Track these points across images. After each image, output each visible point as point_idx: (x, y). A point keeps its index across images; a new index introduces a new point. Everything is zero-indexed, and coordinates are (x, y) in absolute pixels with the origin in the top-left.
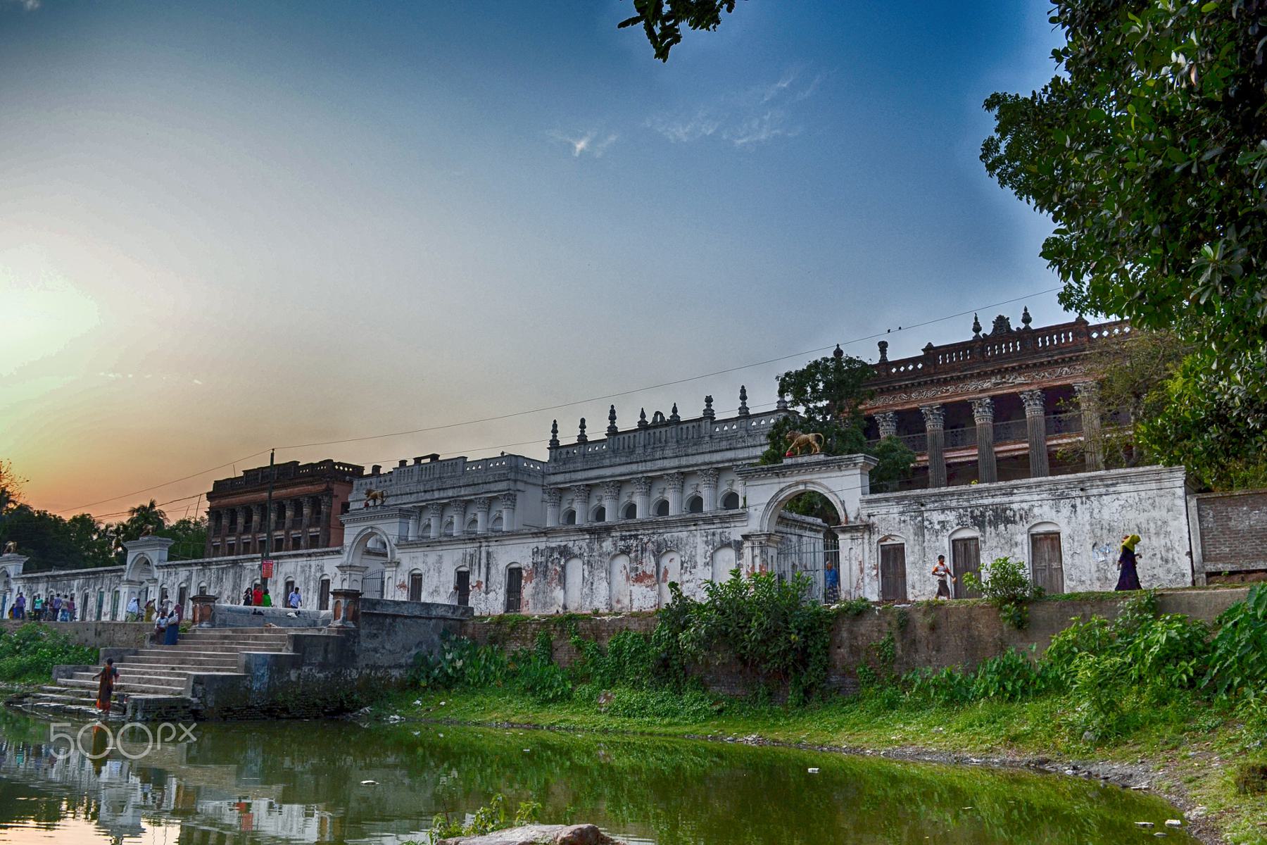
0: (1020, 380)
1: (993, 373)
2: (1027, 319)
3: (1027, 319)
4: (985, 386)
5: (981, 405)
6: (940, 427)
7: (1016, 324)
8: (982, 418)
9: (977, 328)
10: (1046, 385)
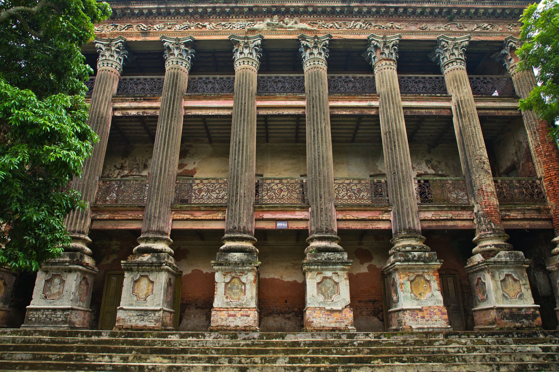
1: (270, 13)
4: (256, 27)
5: (246, 46)
10: (335, 36)
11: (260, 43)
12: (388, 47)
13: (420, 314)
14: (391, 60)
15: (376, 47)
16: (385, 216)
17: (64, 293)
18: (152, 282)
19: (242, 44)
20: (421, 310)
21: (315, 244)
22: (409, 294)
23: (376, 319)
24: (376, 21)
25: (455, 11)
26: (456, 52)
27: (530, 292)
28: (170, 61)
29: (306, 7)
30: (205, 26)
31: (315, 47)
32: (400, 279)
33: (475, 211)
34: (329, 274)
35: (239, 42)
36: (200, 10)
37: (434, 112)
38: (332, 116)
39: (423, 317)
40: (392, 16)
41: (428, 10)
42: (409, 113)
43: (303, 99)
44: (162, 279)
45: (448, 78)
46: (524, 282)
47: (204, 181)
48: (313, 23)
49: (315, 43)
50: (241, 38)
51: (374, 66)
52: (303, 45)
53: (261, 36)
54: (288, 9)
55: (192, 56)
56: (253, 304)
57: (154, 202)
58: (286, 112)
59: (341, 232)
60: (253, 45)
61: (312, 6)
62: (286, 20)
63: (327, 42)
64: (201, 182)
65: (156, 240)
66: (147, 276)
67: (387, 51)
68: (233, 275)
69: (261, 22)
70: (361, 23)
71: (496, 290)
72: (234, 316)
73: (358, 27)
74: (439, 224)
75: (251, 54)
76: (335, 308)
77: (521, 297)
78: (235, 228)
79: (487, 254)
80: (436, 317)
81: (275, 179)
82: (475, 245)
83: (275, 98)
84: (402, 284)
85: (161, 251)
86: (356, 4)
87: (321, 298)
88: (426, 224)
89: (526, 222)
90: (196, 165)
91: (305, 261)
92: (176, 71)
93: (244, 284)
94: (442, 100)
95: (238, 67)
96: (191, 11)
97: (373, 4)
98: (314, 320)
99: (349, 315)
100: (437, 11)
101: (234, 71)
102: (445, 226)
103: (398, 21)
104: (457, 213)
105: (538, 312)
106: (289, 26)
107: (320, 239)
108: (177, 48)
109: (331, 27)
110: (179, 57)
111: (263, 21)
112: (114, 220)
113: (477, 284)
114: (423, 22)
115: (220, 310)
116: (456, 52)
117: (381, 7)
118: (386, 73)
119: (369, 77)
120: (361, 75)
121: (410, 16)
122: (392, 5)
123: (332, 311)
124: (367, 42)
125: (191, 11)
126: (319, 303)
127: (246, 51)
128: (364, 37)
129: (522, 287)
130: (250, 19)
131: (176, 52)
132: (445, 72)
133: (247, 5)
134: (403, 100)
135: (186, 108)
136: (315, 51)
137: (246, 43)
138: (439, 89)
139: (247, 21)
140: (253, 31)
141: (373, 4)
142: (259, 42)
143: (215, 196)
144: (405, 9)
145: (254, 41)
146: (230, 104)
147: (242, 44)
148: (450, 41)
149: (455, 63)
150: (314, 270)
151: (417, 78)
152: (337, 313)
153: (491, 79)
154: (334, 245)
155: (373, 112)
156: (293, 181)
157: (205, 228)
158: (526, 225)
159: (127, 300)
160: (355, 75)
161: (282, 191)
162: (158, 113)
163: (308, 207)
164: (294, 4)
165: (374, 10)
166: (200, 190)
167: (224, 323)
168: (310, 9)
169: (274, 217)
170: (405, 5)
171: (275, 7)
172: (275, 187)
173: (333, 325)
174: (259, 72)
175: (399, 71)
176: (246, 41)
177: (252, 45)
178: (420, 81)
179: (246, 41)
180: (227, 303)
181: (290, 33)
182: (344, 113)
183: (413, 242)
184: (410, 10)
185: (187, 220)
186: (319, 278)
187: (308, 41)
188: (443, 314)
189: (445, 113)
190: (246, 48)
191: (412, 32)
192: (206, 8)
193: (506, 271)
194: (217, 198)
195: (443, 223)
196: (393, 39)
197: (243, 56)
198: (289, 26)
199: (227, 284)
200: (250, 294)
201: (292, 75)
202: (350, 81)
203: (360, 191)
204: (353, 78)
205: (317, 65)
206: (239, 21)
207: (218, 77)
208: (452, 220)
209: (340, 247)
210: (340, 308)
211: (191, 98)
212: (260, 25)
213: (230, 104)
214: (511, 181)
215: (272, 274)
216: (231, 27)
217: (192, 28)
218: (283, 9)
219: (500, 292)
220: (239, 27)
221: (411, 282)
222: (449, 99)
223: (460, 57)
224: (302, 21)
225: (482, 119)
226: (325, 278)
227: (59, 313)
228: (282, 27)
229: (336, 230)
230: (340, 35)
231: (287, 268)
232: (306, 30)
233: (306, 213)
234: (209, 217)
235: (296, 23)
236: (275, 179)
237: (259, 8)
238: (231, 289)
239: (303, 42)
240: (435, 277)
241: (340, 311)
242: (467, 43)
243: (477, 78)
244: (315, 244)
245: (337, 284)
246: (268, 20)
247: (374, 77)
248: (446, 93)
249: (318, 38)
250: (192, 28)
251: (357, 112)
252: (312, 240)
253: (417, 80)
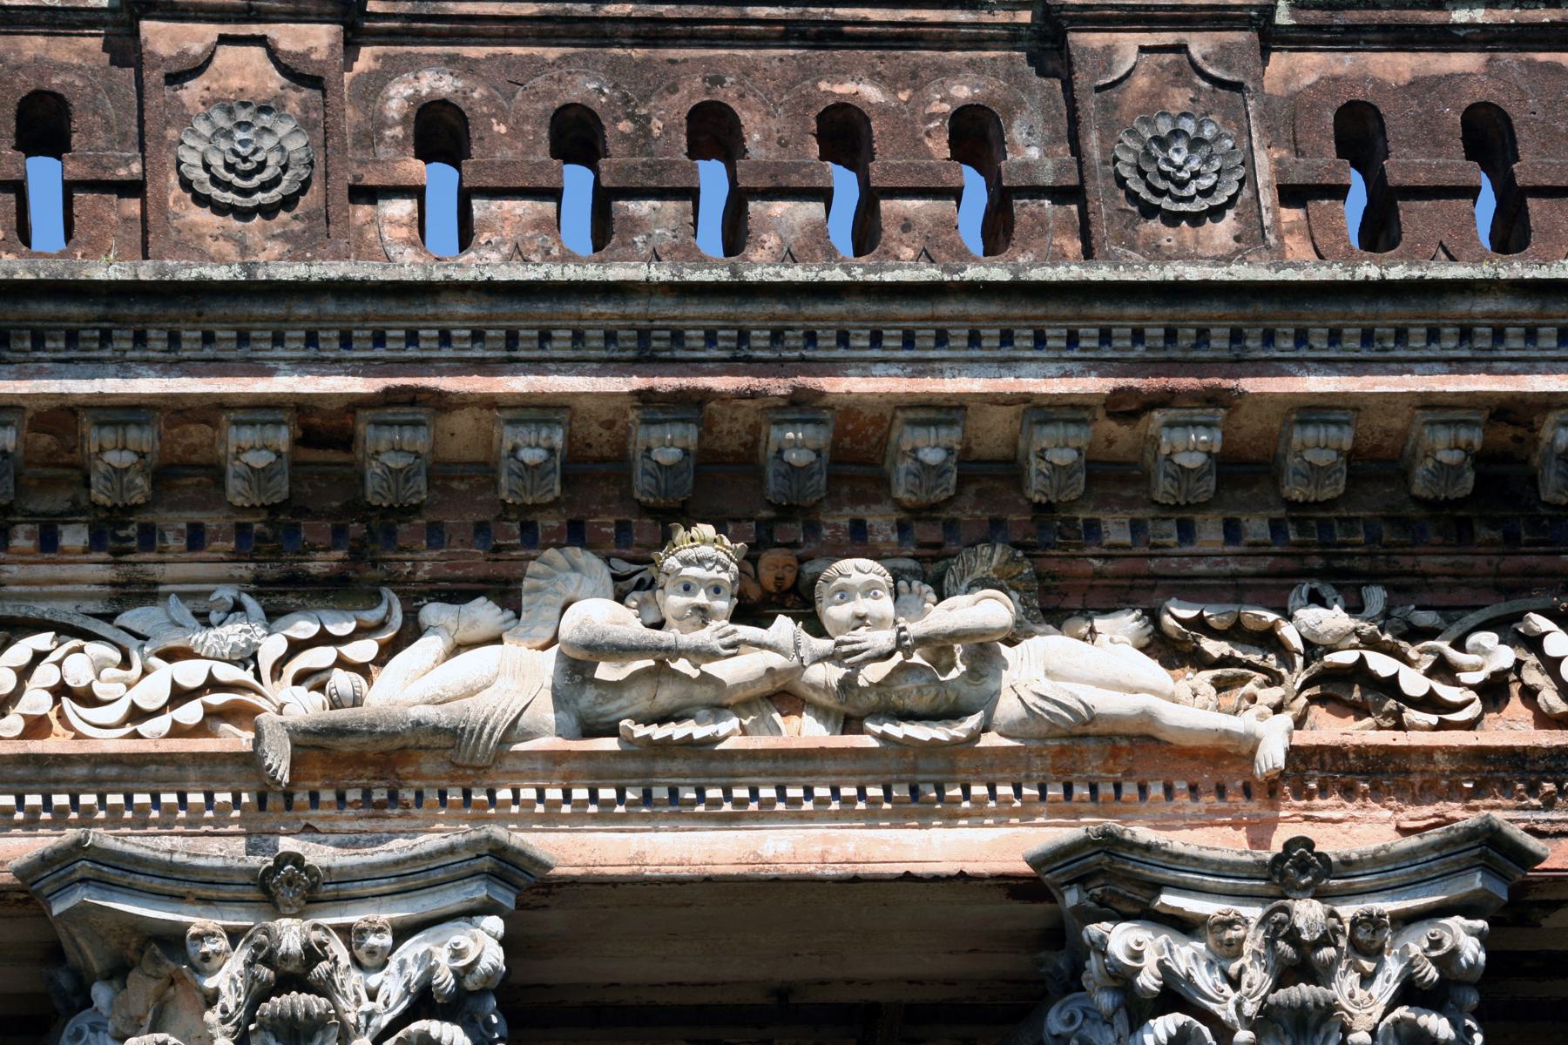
0: (1097, 667)
11: (492, 956)
29: (1123, 407)
35: (173, 941)
48: (1236, 633)
52: (1122, 979)
53: (506, 866)
60: (393, 986)
61: (1213, 398)
63: (1465, 938)
69: (484, 614)
109: (1494, 691)
111: (507, 595)
130: (318, 565)
139: (259, 587)
142: (484, 944)
145: (402, 932)
147: (228, 977)
171: (691, 404)
176: (291, 934)
179: (291, 934)
187: (1185, 926)
212: (472, 674)
216: (36, 700)
218: (797, 442)
220: (152, 692)
237: (462, 422)
239: (1121, 938)
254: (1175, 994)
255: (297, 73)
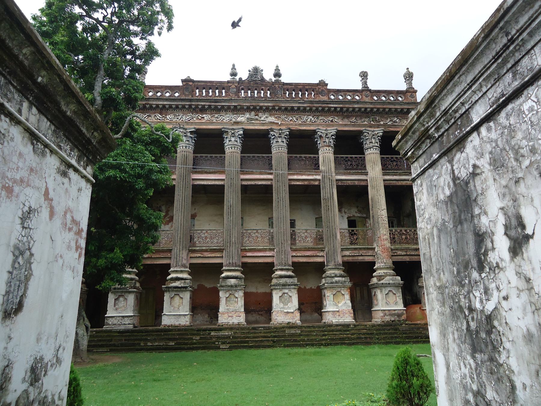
0: (272, 119)
1: (249, 109)
2: (277, 74)
3: (277, 74)
4: (239, 119)
5: (233, 135)
6: (191, 149)
7: (268, 76)
8: (232, 146)
9: (234, 74)
10: (294, 128)
12: (328, 138)
13: (338, 314)
14: (329, 146)
15: (321, 136)
16: (321, 254)
17: (128, 306)
18: (182, 298)
19: (230, 134)
20: (338, 311)
21: (279, 273)
22: (332, 303)
23: (316, 314)
24: (322, 116)
25: (375, 110)
26: (373, 141)
27: (402, 300)
28: (181, 145)
29: (274, 106)
30: (203, 118)
31: (280, 137)
32: (328, 294)
33: (376, 250)
34: (286, 291)
36: (200, 107)
37: (356, 183)
38: (291, 186)
39: (339, 316)
40: (332, 112)
41: (357, 109)
42: (340, 184)
43: (271, 174)
44: (187, 296)
45: (368, 158)
46: (399, 295)
47: (209, 231)
49: (280, 134)
50: (229, 129)
51: (318, 150)
54: (261, 108)
55: (195, 140)
56: (243, 310)
57: (178, 247)
58: (260, 183)
59: (294, 264)
62: (260, 114)
64: (207, 232)
65: (182, 272)
66: (178, 295)
67: (327, 140)
68: (231, 292)
70: (311, 117)
71: (383, 299)
72: (232, 317)
73: (309, 120)
74: (354, 258)
75: (236, 141)
76: (289, 311)
77: (396, 303)
78: (230, 263)
79: (380, 278)
80: (347, 315)
81: (254, 230)
82: (375, 271)
83: (252, 173)
84: (328, 296)
85: (186, 279)
86: (308, 105)
87: (282, 305)
88: (346, 259)
89: (407, 257)
90: (196, 210)
91: (272, 284)
92: (185, 153)
93: (237, 298)
94: (362, 174)
95: (228, 150)
96: (193, 107)
97: (320, 105)
98: (278, 318)
99: (298, 315)
100: (363, 109)
101: (225, 152)
102: (358, 259)
103: (337, 116)
104: (365, 251)
105: (405, 312)
106: (262, 119)
107: (282, 270)
108: (185, 136)
110: (187, 142)
111: (244, 114)
112: (151, 258)
113: (374, 295)
114: (354, 116)
115: (223, 314)
116: (373, 141)
117: (325, 107)
118: (326, 154)
119: (315, 157)
120: (310, 155)
121: (344, 112)
122: (332, 106)
123: (288, 313)
124: (314, 132)
125: (193, 107)
126: (281, 308)
127: (233, 139)
128: (312, 128)
129: (397, 298)
131: (184, 139)
132: (366, 154)
133: (233, 104)
134: (337, 174)
135: (193, 179)
136: (280, 140)
137: (233, 134)
138: (360, 166)
140: (237, 123)
141: (320, 105)
142: (242, 132)
143: (216, 241)
144: (342, 108)
146: (222, 177)
148: (370, 133)
149: (372, 149)
150: (277, 289)
151: (347, 157)
152: (291, 314)
153: (396, 158)
154: (290, 273)
155: (317, 183)
156: (265, 231)
157: (211, 262)
158: (407, 259)
159: (166, 310)
160: (306, 155)
161: (258, 237)
162: (174, 183)
163: (274, 249)
164: (266, 104)
165: (320, 108)
166: (206, 238)
167: (226, 321)
168: (277, 108)
169: (253, 255)
170: (341, 106)
171: (253, 106)
172: (254, 235)
173: (288, 321)
174: (242, 153)
175: (335, 153)
177: (237, 134)
178: (349, 160)
180: (228, 309)
181: (263, 124)
182: (298, 183)
183: (337, 272)
184: (345, 109)
185: (199, 257)
186: (280, 294)
188: (351, 314)
189: (363, 183)
190: (233, 136)
191: (345, 125)
192: (204, 105)
193: (389, 289)
194: (217, 243)
195: (356, 258)
196: (332, 131)
197: (231, 143)
198: (262, 119)
199: (227, 298)
200: (241, 303)
201: (264, 155)
202: (303, 160)
203: (306, 237)
204: (305, 157)
205: (280, 151)
206: (227, 114)
207: (214, 155)
208: (362, 255)
209: (293, 274)
210: (293, 311)
211: (196, 172)
212: (241, 118)
213: (222, 177)
214: (401, 231)
215: (252, 289)
217: (195, 119)
218: (258, 107)
219: (385, 301)
221: (334, 295)
222: (366, 174)
223: (376, 145)
224: (270, 115)
225: (386, 187)
226: (284, 293)
227: (126, 319)
228: (257, 120)
229: (290, 263)
230: (296, 127)
231: (260, 282)
232: (274, 123)
233: (273, 252)
234: (213, 255)
235: (267, 117)
236: (254, 230)
238: (229, 301)
239: (272, 133)
240: (347, 293)
241: (292, 313)
242: (381, 134)
243: (387, 158)
244: (279, 273)
245: (291, 297)
246: (248, 115)
247: (318, 157)
248: (366, 169)
249: (281, 130)
250: (195, 119)
251: (306, 183)
252: (276, 270)
253: (347, 159)
254: (274, 135)
255: (236, 86)
